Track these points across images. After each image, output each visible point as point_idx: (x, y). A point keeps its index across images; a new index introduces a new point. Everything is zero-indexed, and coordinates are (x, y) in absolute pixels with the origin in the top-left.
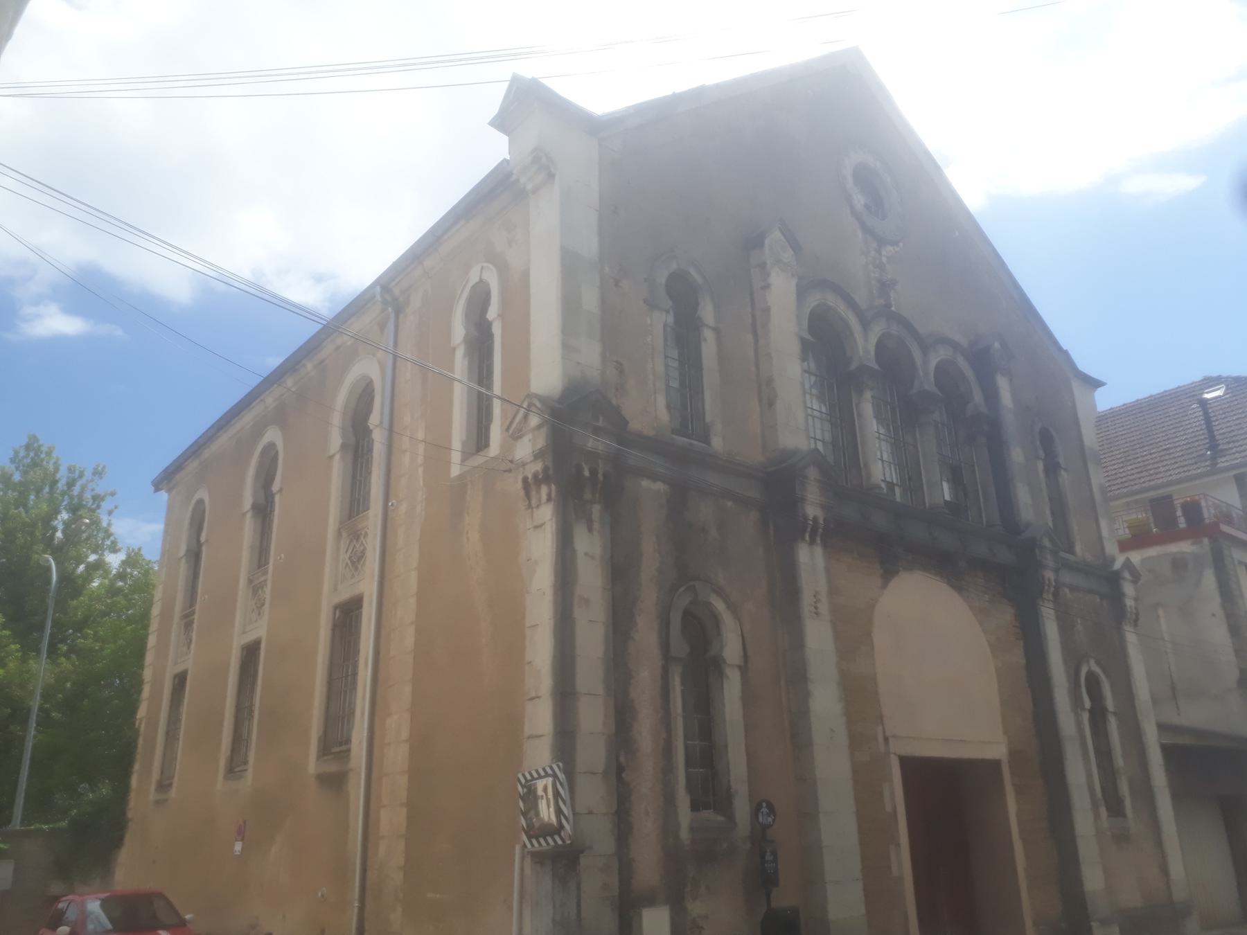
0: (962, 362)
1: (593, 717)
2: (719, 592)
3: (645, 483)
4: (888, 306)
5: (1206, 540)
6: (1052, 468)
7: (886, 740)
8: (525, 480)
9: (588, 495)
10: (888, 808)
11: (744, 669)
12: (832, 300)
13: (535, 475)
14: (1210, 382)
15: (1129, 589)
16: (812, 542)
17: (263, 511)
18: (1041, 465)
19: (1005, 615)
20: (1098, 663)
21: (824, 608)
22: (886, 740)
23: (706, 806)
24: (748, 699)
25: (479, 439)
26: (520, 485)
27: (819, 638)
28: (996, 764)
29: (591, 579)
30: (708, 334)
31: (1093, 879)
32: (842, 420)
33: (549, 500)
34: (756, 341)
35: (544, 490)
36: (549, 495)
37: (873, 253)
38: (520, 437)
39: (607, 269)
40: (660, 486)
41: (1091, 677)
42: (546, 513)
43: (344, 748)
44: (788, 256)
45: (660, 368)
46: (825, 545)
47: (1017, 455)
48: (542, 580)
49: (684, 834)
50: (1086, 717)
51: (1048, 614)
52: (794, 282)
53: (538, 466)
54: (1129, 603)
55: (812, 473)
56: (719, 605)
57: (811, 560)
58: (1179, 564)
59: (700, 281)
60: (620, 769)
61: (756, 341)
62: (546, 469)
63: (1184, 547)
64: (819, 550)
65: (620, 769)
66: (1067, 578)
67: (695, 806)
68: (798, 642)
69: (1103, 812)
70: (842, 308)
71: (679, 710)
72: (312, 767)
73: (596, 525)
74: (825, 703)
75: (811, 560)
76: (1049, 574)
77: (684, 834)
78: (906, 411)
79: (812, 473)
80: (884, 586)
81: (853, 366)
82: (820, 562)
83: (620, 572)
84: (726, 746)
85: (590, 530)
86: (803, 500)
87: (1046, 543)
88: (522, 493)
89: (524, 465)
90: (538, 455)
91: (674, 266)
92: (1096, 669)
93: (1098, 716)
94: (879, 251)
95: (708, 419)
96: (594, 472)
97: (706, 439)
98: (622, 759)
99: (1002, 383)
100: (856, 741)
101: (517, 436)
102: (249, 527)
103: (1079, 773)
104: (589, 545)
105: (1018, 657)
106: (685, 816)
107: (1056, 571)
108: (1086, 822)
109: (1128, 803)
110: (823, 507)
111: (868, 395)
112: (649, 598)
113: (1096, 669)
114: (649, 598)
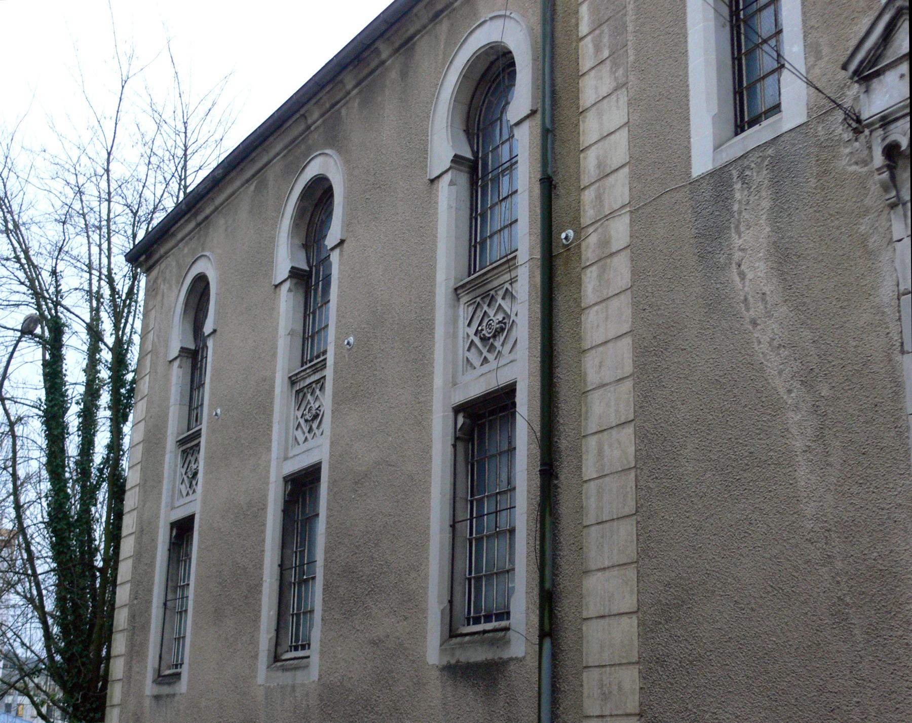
26: (879, 160)
38: (878, 74)
43: (503, 623)
72: (433, 652)
88: (886, 175)
101: (867, 74)
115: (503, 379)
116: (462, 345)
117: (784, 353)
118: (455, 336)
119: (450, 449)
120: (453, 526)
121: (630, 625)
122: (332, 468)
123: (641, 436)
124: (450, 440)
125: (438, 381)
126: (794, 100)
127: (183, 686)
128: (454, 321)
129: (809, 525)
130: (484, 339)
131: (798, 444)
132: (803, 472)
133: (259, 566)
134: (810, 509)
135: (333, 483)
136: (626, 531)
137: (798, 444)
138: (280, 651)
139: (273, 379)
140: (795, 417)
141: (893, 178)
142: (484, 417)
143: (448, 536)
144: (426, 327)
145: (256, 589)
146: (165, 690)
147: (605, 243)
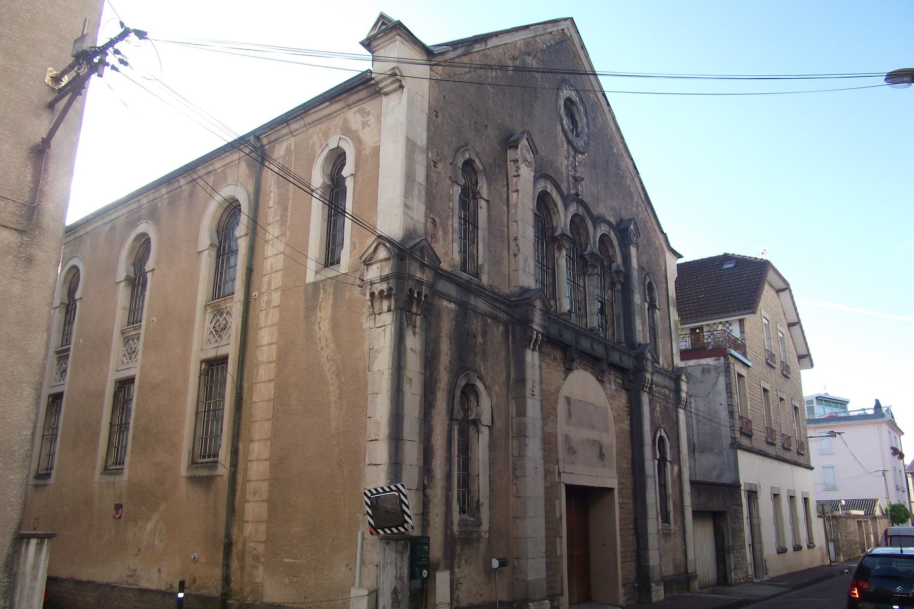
0: (613, 235)
1: (412, 453)
2: (481, 378)
3: (445, 303)
4: (577, 195)
5: (722, 359)
6: (652, 306)
7: (559, 474)
8: (372, 295)
9: (414, 310)
10: (558, 516)
11: (491, 428)
12: (550, 188)
13: (382, 292)
14: (726, 257)
15: (684, 386)
16: (534, 350)
17: (137, 283)
18: (646, 305)
19: (622, 399)
20: (665, 431)
21: (537, 391)
22: (559, 474)
23: (464, 512)
24: (492, 446)
25: (331, 258)
26: (368, 297)
27: (533, 408)
28: (611, 490)
29: (414, 364)
30: (483, 203)
31: (654, 558)
32: (547, 267)
33: (389, 310)
34: (508, 213)
35: (385, 304)
36: (389, 307)
37: (571, 159)
38: (371, 264)
39: (430, 154)
40: (452, 305)
41: (661, 437)
42: (387, 319)
44: (530, 157)
45: (456, 225)
46: (540, 352)
47: (637, 298)
48: (383, 362)
49: (456, 528)
50: (656, 462)
51: (645, 398)
52: (533, 174)
53: (384, 286)
54: (684, 395)
55: (538, 304)
56: (480, 385)
57: (532, 358)
58: (705, 370)
59: (481, 168)
60: (425, 488)
61: (508, 213)
62: (390, 289)
63: (710, 361)
64: (536, 354)
65: (425, 488)
66: (657, 378)
67: (462, 511)
68: (522, 412)
69: (660, 518)
70: (555, 195)
71: (456, 453)
72: (183, 470)
73: (417, 330)
74: (534, 449)
75: (532, 358)
76: (648, 376)
77: (456, 528)
78: (582, 263)
79: (538, 304)
80: (565, 379)
81: (558, 233)
82: (537, 362)
83: (429, 361)
84: (478, 476)
85: (414, 333)
86: (532, 321)
87: (649, 356)
88: (370, 303)
89: (372, 283)
90: (384, 279)
91: (468, 156)
92: (664, 434)
93: (662, 461)
94: (574, 157)
95: (480, 262)
96: (419, 294)
97: (477, 275)
98: (426, 482)
99: (633, 250)
100: (547, 473)
101: (368, 263)
102: (123, 295)
103: (652, 496)
104: (413, 342)
105: (626, 426)
106: (456, 517)
107: (652, 374)
108: (653, 524)
109: (672, 515)
110: (543, 326)
111: (564, 252)
112: (444, 378)
113: (664, 434)
114: (444, 378)
115: (222, 352)
116: (206, 332)
117: (331, 363)
118: (203, 327)
119: (197, 379)
120: (197, 414)
121: (266, 465)
122: (141, 380)
123: (277, 387)
124: (198, 375)
125: (195, 347)
126: (346, 256)
127: (52, 480)
128: (204, 320)
129: (333, 431)
130: (216, 331)
131: (332, 399)
132: (333, 409)
133: (99, 422)
134: (334, 425)
135: (140, 387)
136: (267, 425)
137: (332, 399)
138: (108, 465)
139: (112, 331)
140: (332, 388)
141: (372, 304)
142: (214, 366)
143: (194, 418)
144: (190, 320)
145: (97, 434)
146: (41, 482)
147: (269, 302)
